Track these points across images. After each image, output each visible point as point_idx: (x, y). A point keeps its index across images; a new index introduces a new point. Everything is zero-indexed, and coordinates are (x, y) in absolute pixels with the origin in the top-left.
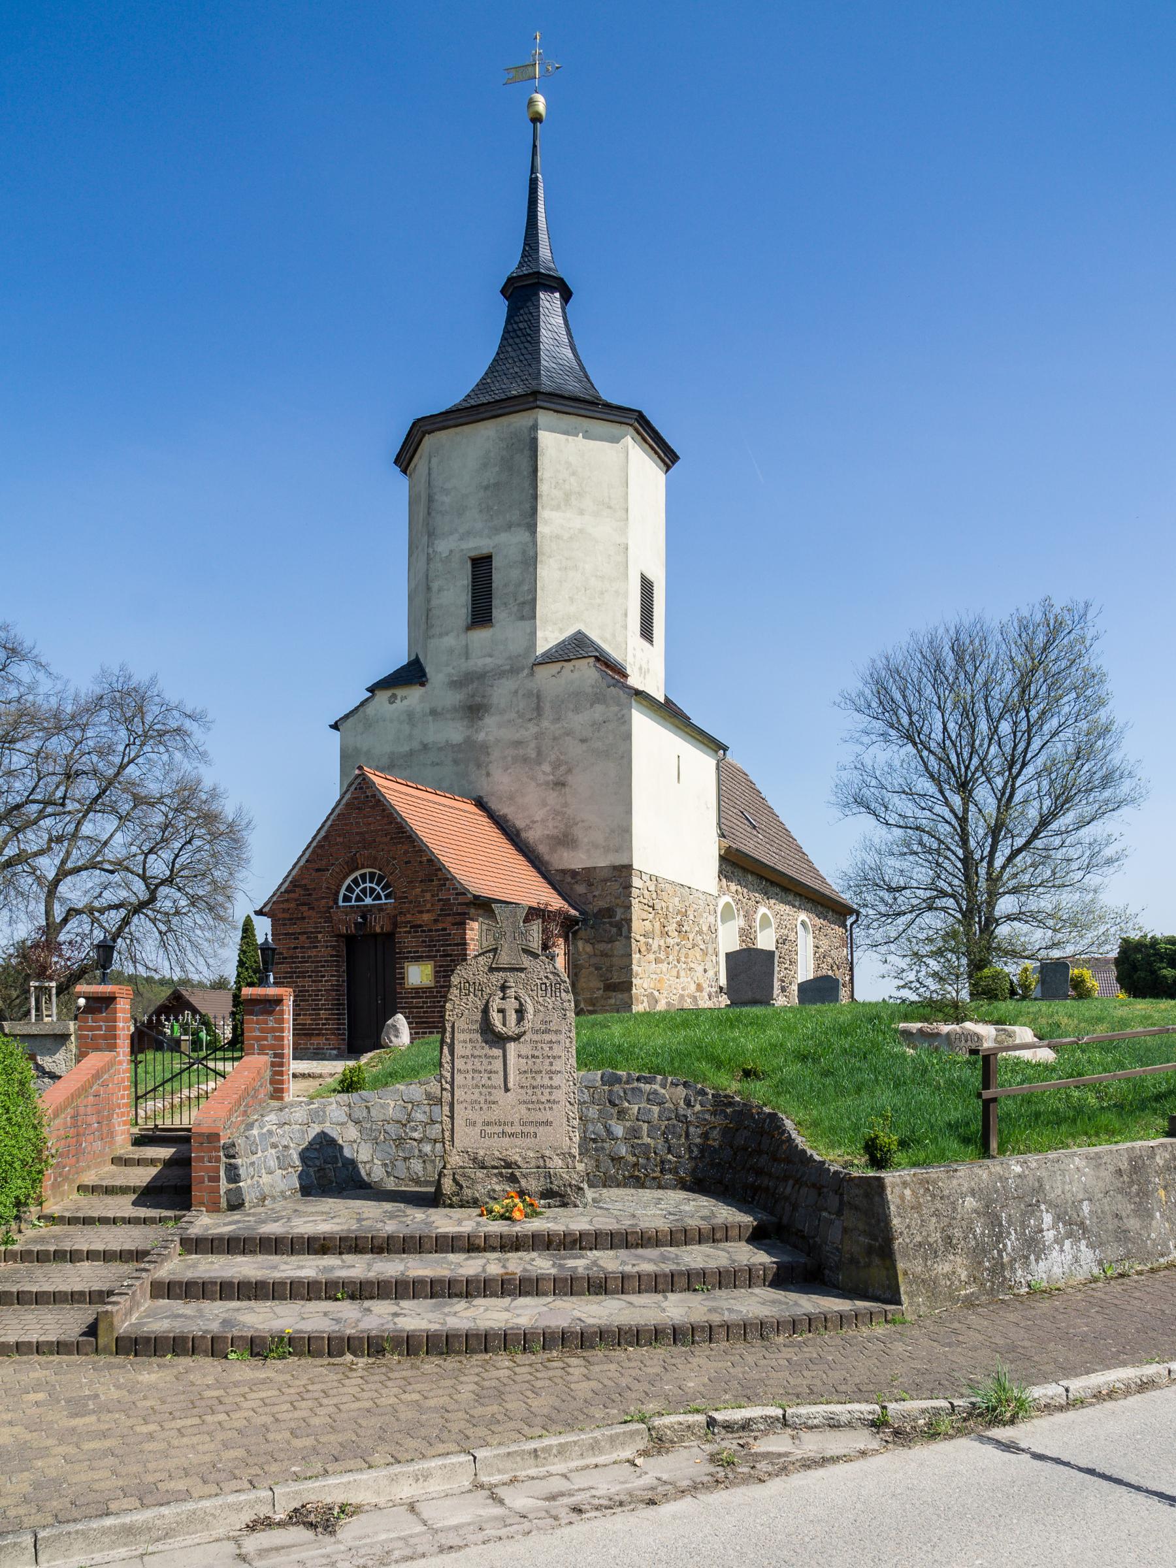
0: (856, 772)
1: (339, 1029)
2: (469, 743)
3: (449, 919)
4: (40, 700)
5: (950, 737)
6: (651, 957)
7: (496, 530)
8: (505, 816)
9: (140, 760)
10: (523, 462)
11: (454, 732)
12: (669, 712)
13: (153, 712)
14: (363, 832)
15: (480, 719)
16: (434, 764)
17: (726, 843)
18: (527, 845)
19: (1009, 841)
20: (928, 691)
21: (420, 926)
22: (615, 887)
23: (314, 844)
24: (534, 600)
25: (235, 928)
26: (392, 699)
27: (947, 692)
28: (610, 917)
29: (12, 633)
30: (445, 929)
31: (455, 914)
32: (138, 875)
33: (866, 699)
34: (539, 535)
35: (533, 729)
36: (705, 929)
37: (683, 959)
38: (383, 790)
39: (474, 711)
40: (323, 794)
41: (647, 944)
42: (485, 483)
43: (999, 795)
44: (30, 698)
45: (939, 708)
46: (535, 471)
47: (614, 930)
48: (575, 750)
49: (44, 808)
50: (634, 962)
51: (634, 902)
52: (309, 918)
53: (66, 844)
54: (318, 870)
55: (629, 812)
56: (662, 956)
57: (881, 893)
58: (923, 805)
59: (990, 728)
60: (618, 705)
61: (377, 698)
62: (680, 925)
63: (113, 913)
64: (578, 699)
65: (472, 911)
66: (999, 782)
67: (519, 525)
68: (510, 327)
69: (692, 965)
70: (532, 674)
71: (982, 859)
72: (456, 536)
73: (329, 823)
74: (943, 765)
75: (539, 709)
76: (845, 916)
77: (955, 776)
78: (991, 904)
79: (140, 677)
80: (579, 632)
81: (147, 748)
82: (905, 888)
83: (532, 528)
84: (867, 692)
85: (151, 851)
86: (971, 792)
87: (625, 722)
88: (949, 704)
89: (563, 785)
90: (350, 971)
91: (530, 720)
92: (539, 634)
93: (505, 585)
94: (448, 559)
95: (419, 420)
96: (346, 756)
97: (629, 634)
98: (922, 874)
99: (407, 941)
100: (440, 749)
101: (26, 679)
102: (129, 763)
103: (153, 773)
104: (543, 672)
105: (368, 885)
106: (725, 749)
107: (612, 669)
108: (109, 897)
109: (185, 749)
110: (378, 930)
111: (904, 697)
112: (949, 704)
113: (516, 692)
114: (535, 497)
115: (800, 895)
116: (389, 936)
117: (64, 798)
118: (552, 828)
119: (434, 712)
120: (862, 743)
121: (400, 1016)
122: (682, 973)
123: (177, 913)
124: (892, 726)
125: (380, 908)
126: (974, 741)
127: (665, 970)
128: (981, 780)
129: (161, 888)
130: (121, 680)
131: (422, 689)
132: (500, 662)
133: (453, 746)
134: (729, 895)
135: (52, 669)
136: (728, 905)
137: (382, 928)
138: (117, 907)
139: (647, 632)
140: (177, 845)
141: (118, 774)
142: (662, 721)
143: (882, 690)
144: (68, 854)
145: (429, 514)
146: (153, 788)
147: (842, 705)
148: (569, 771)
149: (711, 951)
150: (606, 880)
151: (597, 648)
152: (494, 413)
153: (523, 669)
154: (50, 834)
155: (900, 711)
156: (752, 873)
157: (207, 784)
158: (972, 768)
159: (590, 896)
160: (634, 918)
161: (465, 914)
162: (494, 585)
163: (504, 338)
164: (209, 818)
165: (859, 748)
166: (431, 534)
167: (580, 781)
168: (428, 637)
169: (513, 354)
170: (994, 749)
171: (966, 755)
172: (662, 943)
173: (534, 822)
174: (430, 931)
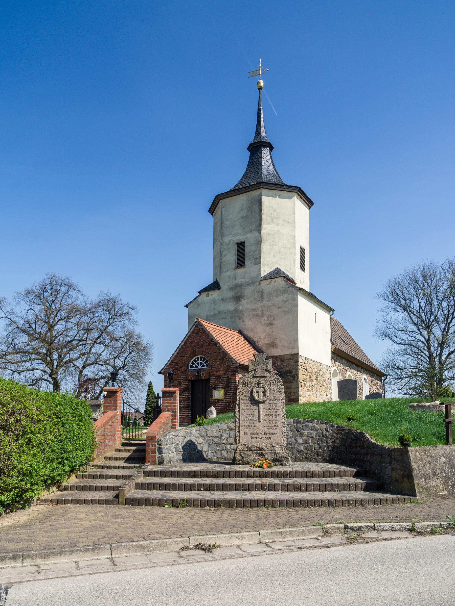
0: (383, 323)
1: (188, 415)
2: (236, 310)
3: (230, 373)
4: (79, 303)
5: (422, 309)
6: (306, 389)
7: (246, 233)
8: (249, 337)
9: (113, 324)
10: (256, 208)
11: (231, 306)
12: (310, 296)
13: (118, 307)
14: (198, 342)
15: (240, 301)
16: (223, 318)
17: (334, 347)
18: (258, 347)
19: (448, 349)
20: (412, 291)
21: (219, 376)
22: (292, 362)
23: (180, 347)
24: (260, 257)
25: (146, 385)
26: (208, 295)
27: (420, 291)
28: (290, 373)
29: (70, 280)
30: (228, 377)
31: (232, 371)
32: (112, 366)
33: (387, 295)
34: (262, 234)
35: (260, 304)
36: (326, 379)
37: (318, 390)
38: (205, 326)
39: (238, 298)
40: (180, 331)
41: (304, 384)
42: (242, 216)
43: (443, 330)
44: (76, 303)
45: (417, 297)
46: (261, 210)
47: (292, 378)
48: (276, 311)
49: (79, 342)
50: (300, 390)
51: (299, 367)
52: (178, 374)
53: (86, 356)
54: (181, 356)
55: (297, 333)
56: (310, 389)
57: (395, 370)
58: (411, 335)
59: (438, 304)
60: (293, 294)
61: (202, 295)
62: (317, 377)
63: (102, 380)
64: (277, 292)
65: (239, 370)
66: (443, 325)
67: (254, 230)
68: (251, 161)
69: (322, 393)
70: (260, 284)
71: (437, 356)
72: (231, 235)
73: (186, 339)
74: (419, 319)
75: (262, 297)
76: (381, 377)
77: (424, 323)
78: (441, 374)
79: (114, 294)
80: (277, 268)
81: (116, 320)
82: (405, 368)
83: (260, 231)
84: (387, 292)
85: (117, 357)
86: (432, 329)
87: (295, 300)
88: (421, 295)
89: (272, 324)
90: (192, 394)
91: (259, 301)
92: (262, 269)
93: (250, 252)
94: (228, 244)
95: (218, 195)
96: (190, 317)
97: (296, 268)
98: (411, 363)
99: (214, 381)
100: (225, 313)
101: (75, 296)
102: (109, 325)
103: (118, 329)
104: (264, 283)
105: (200, 361)
106: (333, 311)
107: (290, 281)
108: (101, 374)
109: (129, 319)
110: (203, 378)
111: (403, 294)
112: (421, 295)
113: (254, 291)
114: (261, 220)
115: (363, 368)
116: (207, 380)
117: (86, 339)
118: (267, 341)
119: (223, 300)
120: (386, 312)
121: (213, 407)
122: (318, 396)
123: (125, 381)
124: (398, 305)
125: (204, 370)
126: (432, 310)
127: (311, 394)
128: (435, 325)
129: (120, 371)
130: (107, 295)
131: (219, 291)
132: (248, 280)
133: (230, 312)
134: (335, 367)
135: (83, 293)
136: (335, 370)
137: (205, 377)
138: (104, 378)
139: (303, 268)
140: (126, 354)
141: (105, 330)
142: (309, 300)
143: (393, 291)
144: (87, 359)
145: (221, 228)
146: (118, 334)
147: (378, 297)
148: (274, 319)
149: (329, 388)
150: (288, 360)
151: (284, 274)
152: (246, 191)
153: (256, 282)
154: (80, 352)
155: (401, 299)
156: (344, 359)
157: (137, 333)
158: (431, 320)
159: (282, 366)
160: (299, 373)
161: (236, 371)
162: (245, 252)
163: (248, 165)
164: (137, 344)
165: (385, 314)
166: (222, 235)
167: (278, 323)
168: (221, 272)
169: (252, 170)
170: (440, 313)
171: (428, 315)
172: (310, 384)
173: (261, 339)
174: (223, 378)
